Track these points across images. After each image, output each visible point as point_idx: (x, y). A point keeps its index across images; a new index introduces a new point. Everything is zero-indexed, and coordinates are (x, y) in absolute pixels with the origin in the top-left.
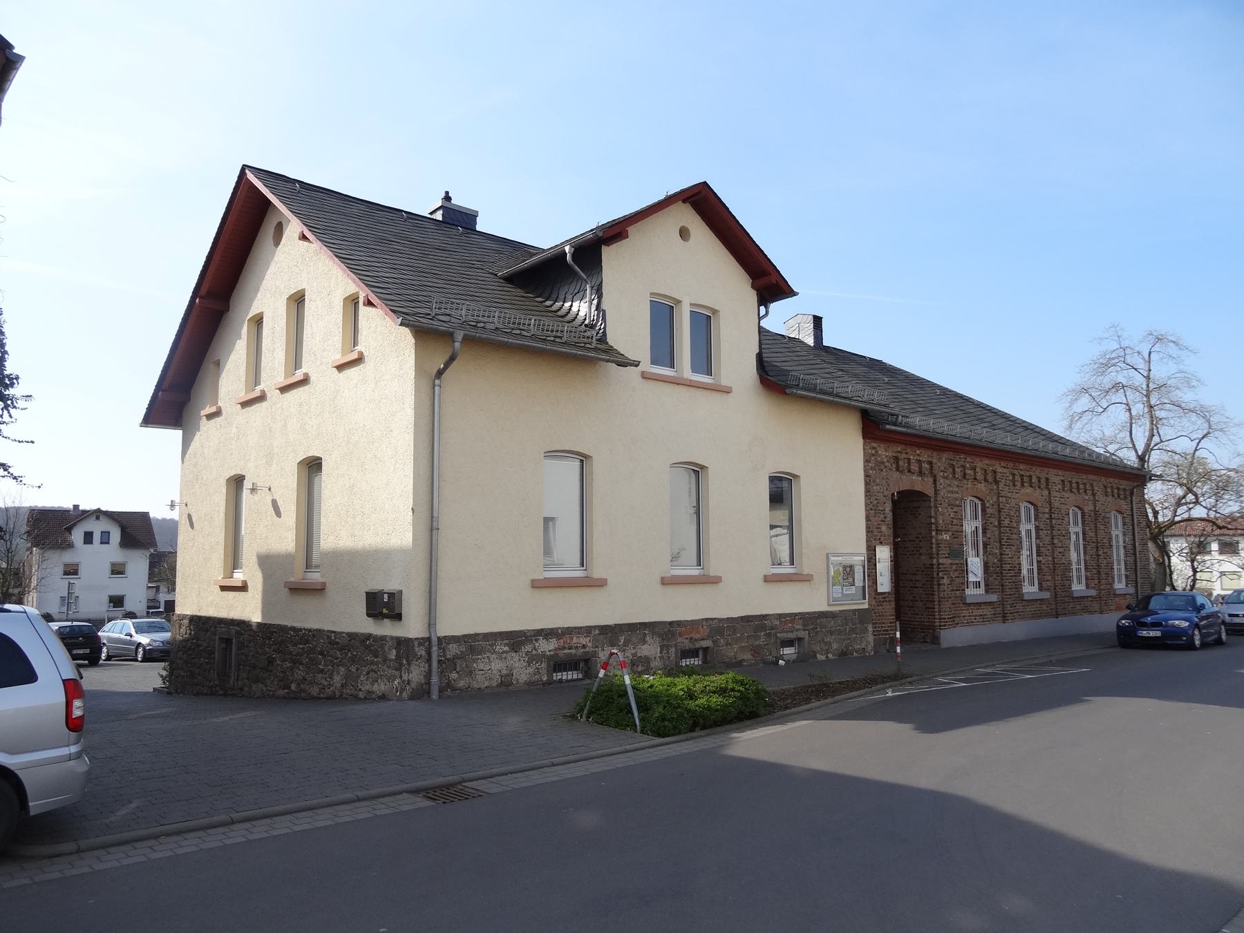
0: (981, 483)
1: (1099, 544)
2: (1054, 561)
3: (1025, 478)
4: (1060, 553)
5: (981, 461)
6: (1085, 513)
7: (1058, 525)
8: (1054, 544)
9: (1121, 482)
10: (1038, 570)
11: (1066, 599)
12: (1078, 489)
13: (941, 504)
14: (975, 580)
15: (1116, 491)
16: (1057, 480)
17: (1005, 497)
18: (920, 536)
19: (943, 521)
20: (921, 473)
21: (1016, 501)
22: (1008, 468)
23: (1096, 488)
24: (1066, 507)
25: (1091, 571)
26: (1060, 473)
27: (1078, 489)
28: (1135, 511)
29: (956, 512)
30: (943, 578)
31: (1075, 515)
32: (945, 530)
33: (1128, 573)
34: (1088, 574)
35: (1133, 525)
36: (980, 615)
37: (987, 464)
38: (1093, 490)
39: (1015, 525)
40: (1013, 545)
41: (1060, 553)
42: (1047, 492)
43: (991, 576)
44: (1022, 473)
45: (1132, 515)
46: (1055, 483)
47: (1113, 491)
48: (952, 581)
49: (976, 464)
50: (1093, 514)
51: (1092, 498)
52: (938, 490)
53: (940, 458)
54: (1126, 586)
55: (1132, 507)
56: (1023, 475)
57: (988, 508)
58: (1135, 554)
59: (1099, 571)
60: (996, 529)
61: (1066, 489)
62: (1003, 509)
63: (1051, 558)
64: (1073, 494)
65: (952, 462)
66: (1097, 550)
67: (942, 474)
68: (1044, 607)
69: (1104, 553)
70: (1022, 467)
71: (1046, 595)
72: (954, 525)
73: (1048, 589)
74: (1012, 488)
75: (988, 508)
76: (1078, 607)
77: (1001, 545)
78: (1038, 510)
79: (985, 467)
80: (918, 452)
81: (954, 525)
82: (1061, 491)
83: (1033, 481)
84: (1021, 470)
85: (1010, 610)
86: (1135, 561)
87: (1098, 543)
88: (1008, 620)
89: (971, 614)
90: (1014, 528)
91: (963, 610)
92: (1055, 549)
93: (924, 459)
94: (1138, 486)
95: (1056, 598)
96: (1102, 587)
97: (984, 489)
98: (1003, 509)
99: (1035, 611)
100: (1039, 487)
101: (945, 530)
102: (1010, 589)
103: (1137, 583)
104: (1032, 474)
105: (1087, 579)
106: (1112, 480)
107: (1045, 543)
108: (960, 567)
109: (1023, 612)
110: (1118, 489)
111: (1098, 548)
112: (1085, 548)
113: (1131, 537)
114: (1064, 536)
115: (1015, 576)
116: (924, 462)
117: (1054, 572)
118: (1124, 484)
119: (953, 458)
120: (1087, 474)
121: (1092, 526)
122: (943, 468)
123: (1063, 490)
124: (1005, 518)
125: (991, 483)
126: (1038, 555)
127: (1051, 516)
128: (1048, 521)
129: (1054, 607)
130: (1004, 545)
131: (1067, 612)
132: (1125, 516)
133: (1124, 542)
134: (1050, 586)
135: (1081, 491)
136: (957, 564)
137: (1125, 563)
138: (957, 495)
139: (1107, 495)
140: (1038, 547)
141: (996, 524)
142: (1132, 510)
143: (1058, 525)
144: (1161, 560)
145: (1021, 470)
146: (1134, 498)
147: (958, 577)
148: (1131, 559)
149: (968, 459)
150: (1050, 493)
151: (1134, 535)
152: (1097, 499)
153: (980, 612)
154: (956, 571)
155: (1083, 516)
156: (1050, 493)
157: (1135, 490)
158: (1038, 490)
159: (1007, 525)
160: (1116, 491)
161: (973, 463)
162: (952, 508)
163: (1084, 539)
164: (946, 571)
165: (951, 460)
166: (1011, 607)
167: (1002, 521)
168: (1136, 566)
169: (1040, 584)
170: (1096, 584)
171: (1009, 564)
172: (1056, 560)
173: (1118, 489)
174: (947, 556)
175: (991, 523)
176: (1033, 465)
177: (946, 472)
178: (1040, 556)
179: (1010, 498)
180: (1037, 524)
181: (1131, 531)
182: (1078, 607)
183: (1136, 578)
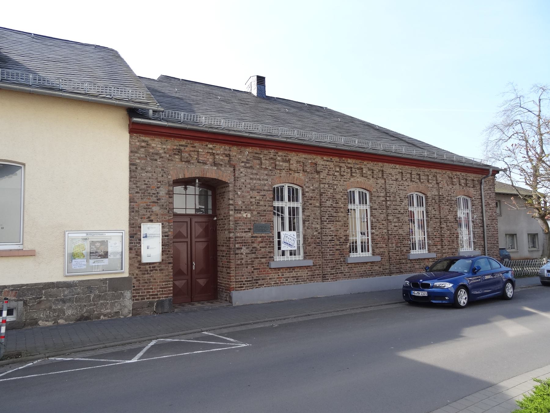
0: (299, 173)
1: (442, 220)
2: (388, 233)
3: (353, 170)
4: (395, 226)
5: (298, 155)
6: (427, 197)
7: (394, 205)
8: (388, 220)
9: (469, 175)
10: (372, 240)
11: (404, 261)
12: (420, 179)
13: (240, 189)
14: (290, 248)
15: (463, 181)
16: (393, 172)
17: (328, 184)
18: (225, 215)
19: (244, 202)
20: (215, 164)
21: (344, 187)
22: (333, 162)
23: (440, 179)
24: (405, 192)
25: (434, 240)
26: (397, 166)
27: (420, 179)
28: (483, 196)
29: (265, 195)
30: (242, 248)
31: (419, 199)
32: (244, 210)
33: (476, 241)
34: (430, 242)
35: (482, 206)
36: (293, 277)
37: (305, 158)
38: (437, 180)
39: (342, 205)
40: (339, 221)
41: (395, 226)
42: (383, 181)
43: (310, 246)
44: (349, 165)
45: (481, 199)
46: (391, 174)
47: (460, 182)
48: (256, 250)
49: (290, 157)
50: (437, 198)
51: (436, 186)
52: (238, 178)
53: (240, 152)
54: (474, 249)
55: (481, 193)
56: (351, 168)
57: (308, 192)
58: (483, 226)
59: (442, 239)
60: (317, 209)
61: (404, 179)
62: (324, 193)
63: (386, 231)
64: (414, 183)
65: (257, 155)
66: (440, 224)
67: (243, 164)
68: (377, 268)
69: (447, 226)
70: (350, 161)
71: (378, 258)
72: (261, 206)
73: (382, 254)
74: (339, 177)
75: (308, 192)
76: (417, 266)
77: (321, 221)
78: (372, 194)
79: (302, 160)
80: (211, 146)
81: (261, 206)
82: (400, 179)
83: (364, 172)
84: (349, 163)
85: (329, 272)
86: (484, 232)
87: (441, 219)
88: (328, 279)
89: (281, 276)
90: (341, 208)
91: (271, 273)
92: (389, 223)
93: (219, 152)
94: (485, 178)
95: (389, 260)
96: (444, 251)
97: (303, 178)
98: (324, 193)
99: (366, 271)
100: (373, 177)
101: (244, 210)
102: (330, 255)
103: (484, 247)
104: (363, 167)
105: (429, 245)
106: (458, 173)
107: (379, 219)
108: (267, 239)
109: (349, 272)
110: (466, 180)
111: (441, 222)
112: (428, 222)
113: (480, 214)
114: (401, 214)
115: (339, 245)
116: (218, 154)
117: (388, 241)
118: (471, 176)
119: (260, 152)
120: (429, 168)
121: (436, 206)
122: (245, 160)
123: (402, 180)
124: (327, 200)
125: (312, 173)
126: (372, 229)
127: (386, 199)
128: (384, 203)
129: (388, 267)
130: (326, 221)
131: (404, 271)
132: (473, 199)
133: (473, 218)
134: (385, 252)
135: (422, 181)
136: (263, 237)
137: (474, 233)
138: (266, 182)
139: (453, 184)
140: (372, 222)
141: (318, 204)
142: (481, 195)
143: (394, 205)
144: (547, 231)
145: (349, 163)
146: (482, 186)
147: (265, 247)
148: (480, 230)
149: (280, 153)
150: (385, 182)
151: (482, 213)
152: (440, 186)
153: (294, 274)
154: (262, 242)
155: (426, 199)
156: (385, 182)
157: (483, 181)
158: (372, 179)
159: (330, 206)
160: (463, 181)
161: (285, 156)
162: (258, 192)
163: (427, 216)
164: (245, 243)
165: (256, 153)
166: (332, 269)
167: (323, 202)
168: (484, 235)
169: (373, 250)
170: (439, 249)
171: (330, 236)
172: (390, 232)
173: (466, 180)
174: (247, 230)
175: (311, 204)
176: (364, 160)
177: (249, 163)
178: (373, 229)
179: (337, 185)
180: (371, 205)
181: (480, 211)
182: (417, 266)
183: (484, 244)
